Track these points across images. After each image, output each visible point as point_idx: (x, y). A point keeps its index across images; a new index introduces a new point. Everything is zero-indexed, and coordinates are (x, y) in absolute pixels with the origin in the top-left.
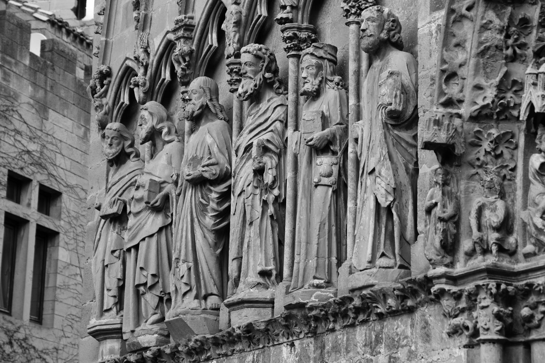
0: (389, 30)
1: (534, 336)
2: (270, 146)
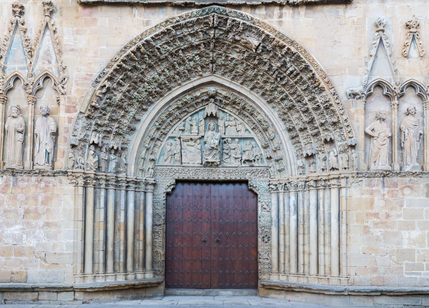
1: (88, 186)
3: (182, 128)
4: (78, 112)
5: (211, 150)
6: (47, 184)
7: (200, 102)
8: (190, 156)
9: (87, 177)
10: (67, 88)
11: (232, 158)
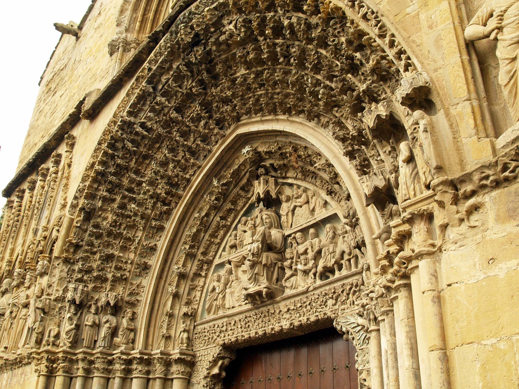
0: (45, 269)
2: (16, 304)
11: (299, 273)
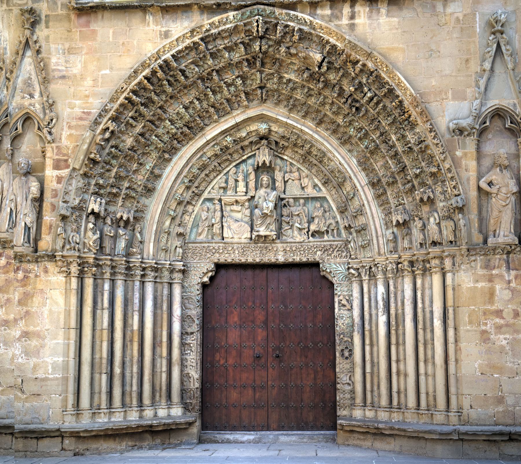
3: (223, 185)
4: (71, 168)
5: (264, 217)
6: (27, 274)
7: (247, 146)
8: (234, 226)
9: (84, 263)
10: (55, 134)
